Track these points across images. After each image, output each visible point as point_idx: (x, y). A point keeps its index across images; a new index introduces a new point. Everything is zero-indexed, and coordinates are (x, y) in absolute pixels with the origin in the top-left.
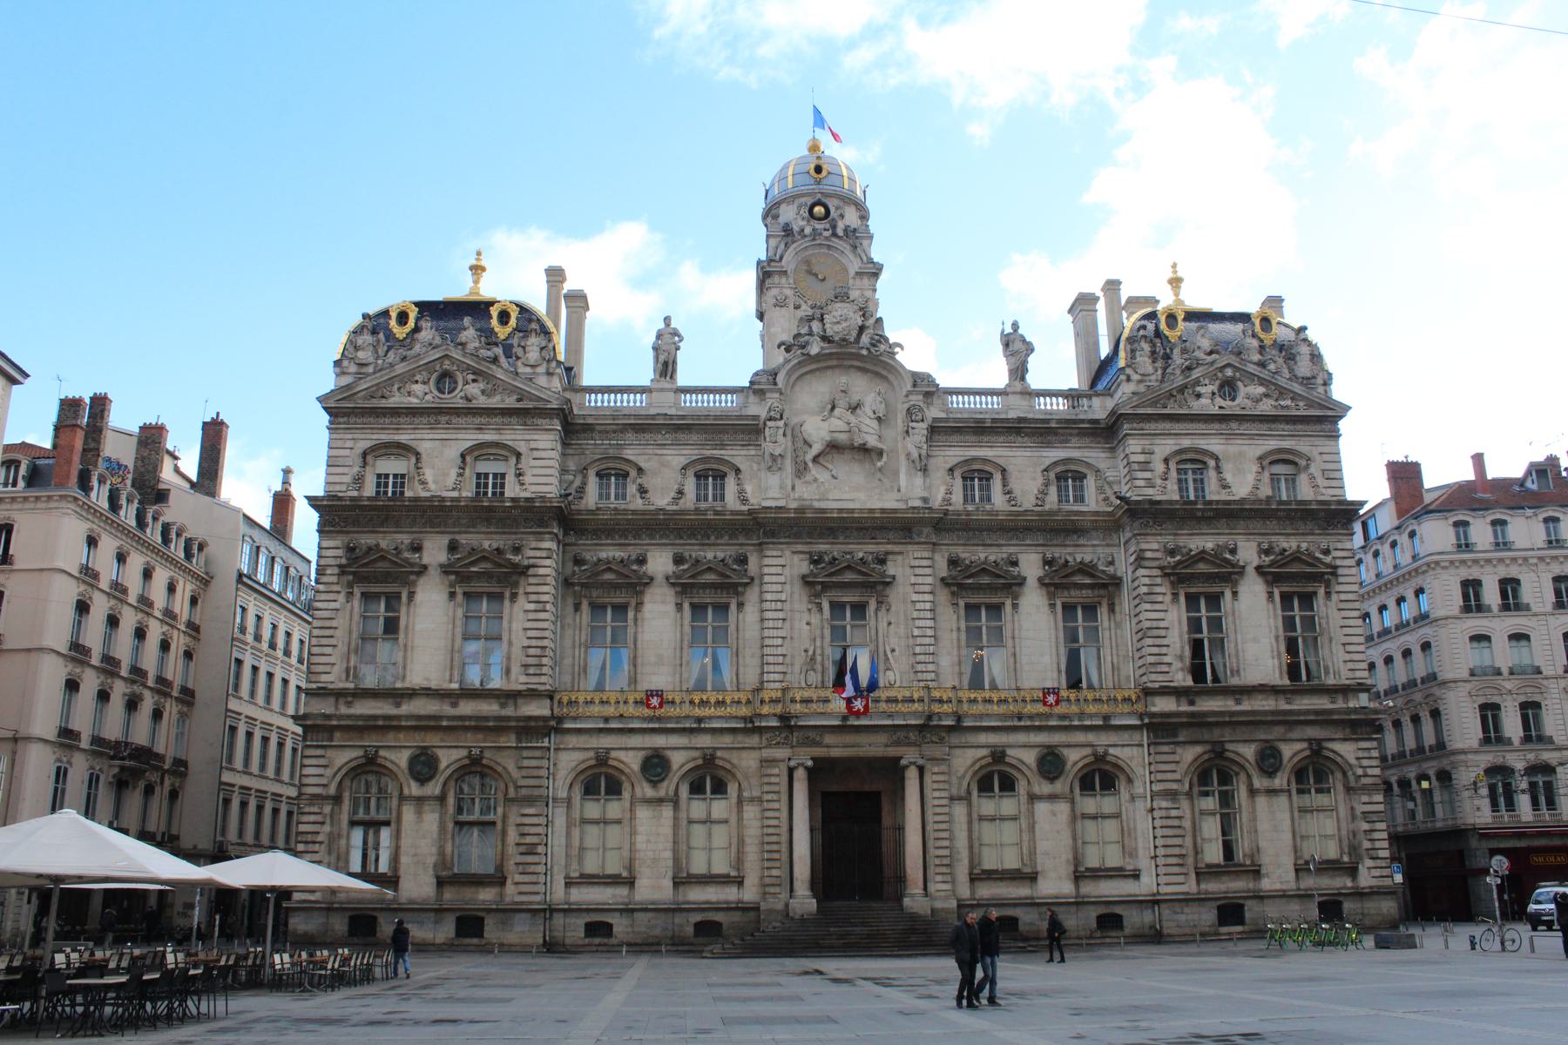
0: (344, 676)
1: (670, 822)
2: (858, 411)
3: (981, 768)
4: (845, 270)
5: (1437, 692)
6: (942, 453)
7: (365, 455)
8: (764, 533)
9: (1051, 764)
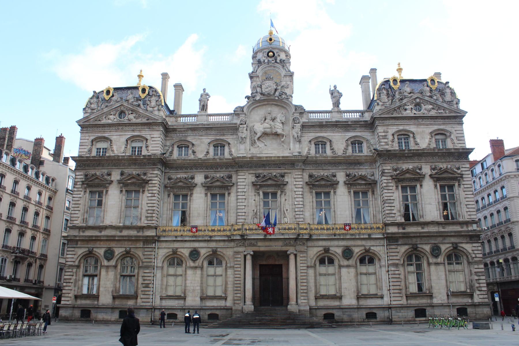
0: (82, 221)
2: (275, 120)
3: (320, 255)
4: (280, 75)
5: (510, 226)
6: (307, 135)
7: (92, 141)
8: (238, 166)
9: (347, 253)
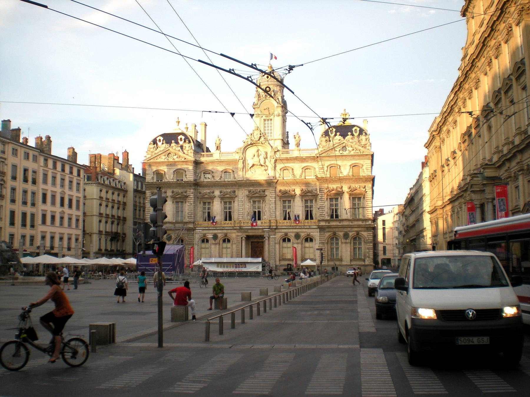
1: (218, 248)
4: (274, 106)
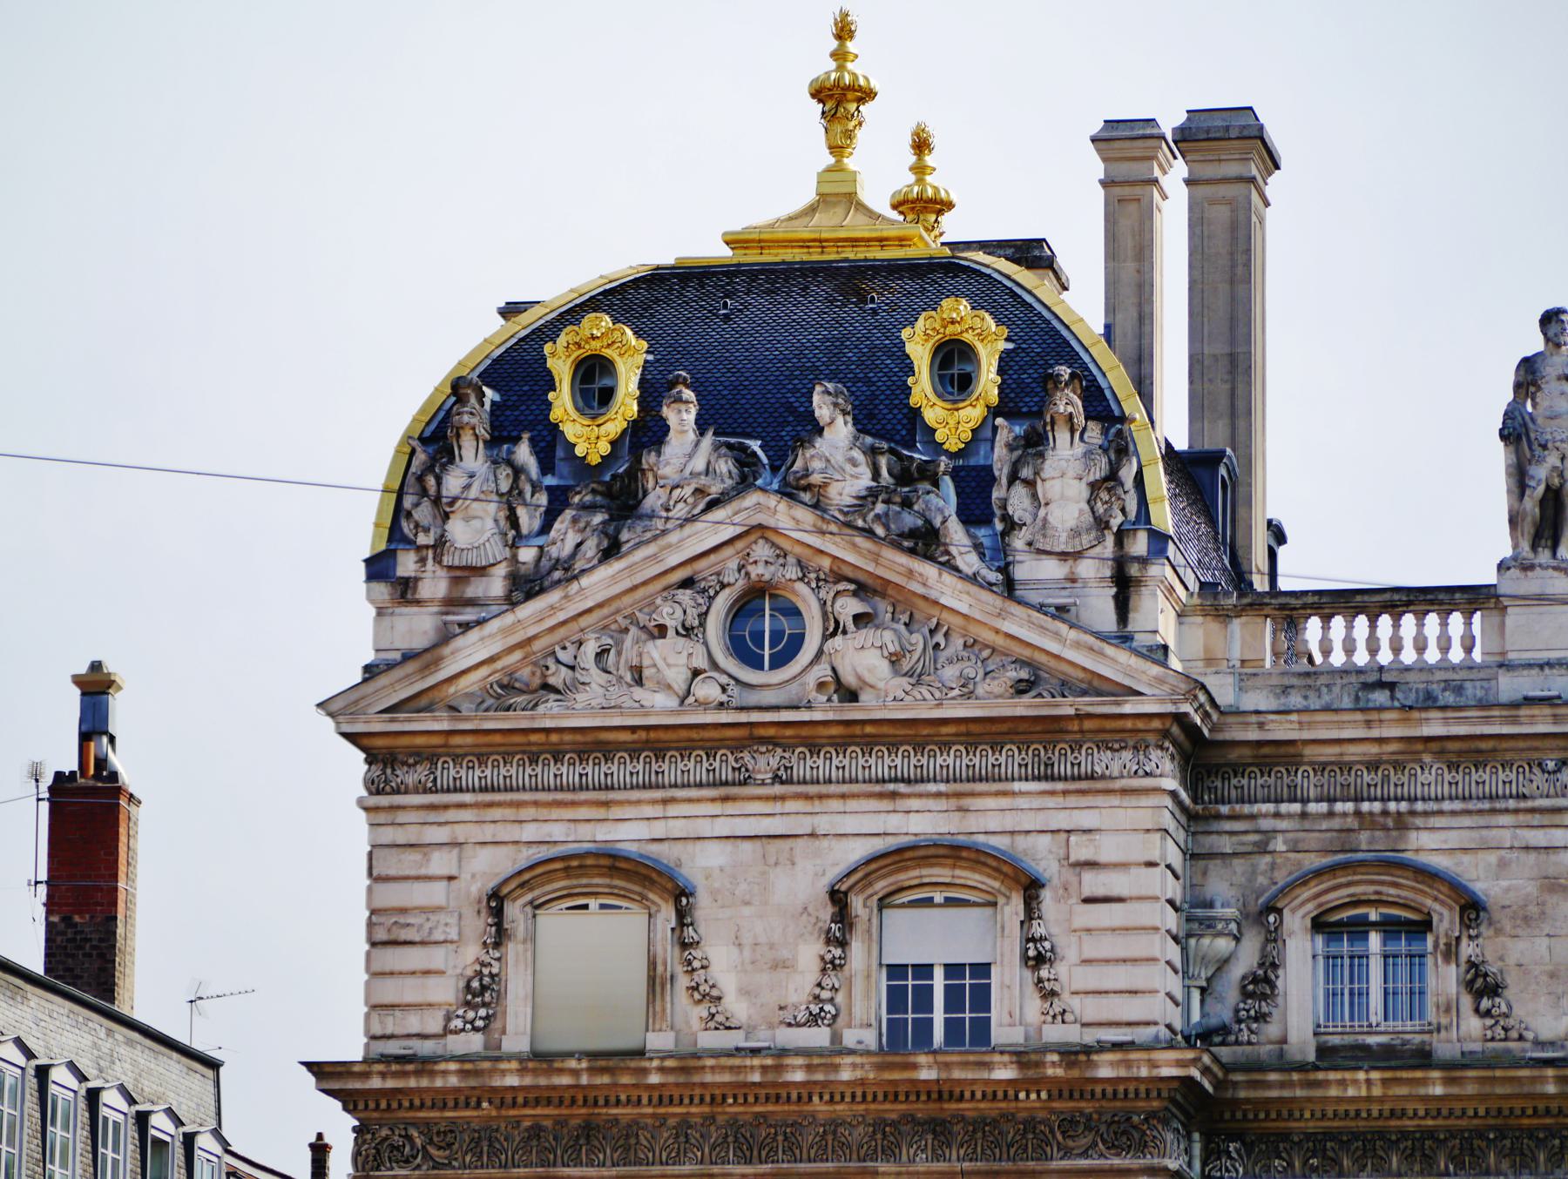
7: (496, 902)
